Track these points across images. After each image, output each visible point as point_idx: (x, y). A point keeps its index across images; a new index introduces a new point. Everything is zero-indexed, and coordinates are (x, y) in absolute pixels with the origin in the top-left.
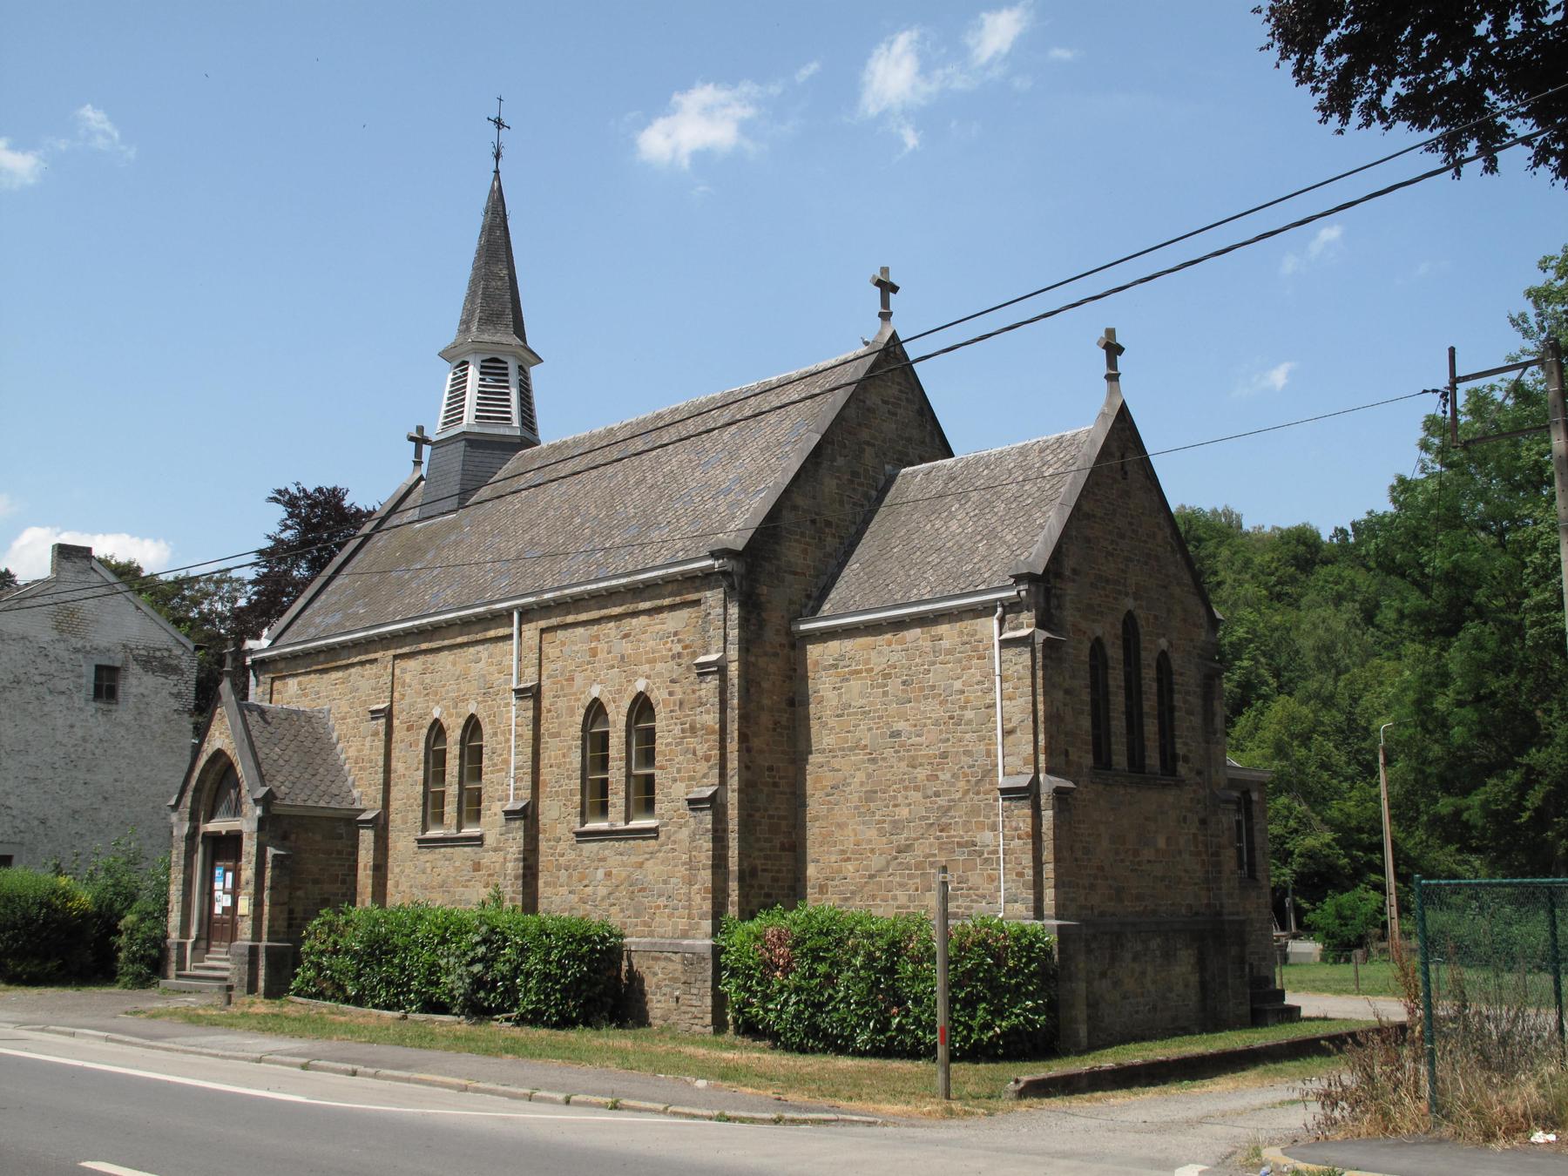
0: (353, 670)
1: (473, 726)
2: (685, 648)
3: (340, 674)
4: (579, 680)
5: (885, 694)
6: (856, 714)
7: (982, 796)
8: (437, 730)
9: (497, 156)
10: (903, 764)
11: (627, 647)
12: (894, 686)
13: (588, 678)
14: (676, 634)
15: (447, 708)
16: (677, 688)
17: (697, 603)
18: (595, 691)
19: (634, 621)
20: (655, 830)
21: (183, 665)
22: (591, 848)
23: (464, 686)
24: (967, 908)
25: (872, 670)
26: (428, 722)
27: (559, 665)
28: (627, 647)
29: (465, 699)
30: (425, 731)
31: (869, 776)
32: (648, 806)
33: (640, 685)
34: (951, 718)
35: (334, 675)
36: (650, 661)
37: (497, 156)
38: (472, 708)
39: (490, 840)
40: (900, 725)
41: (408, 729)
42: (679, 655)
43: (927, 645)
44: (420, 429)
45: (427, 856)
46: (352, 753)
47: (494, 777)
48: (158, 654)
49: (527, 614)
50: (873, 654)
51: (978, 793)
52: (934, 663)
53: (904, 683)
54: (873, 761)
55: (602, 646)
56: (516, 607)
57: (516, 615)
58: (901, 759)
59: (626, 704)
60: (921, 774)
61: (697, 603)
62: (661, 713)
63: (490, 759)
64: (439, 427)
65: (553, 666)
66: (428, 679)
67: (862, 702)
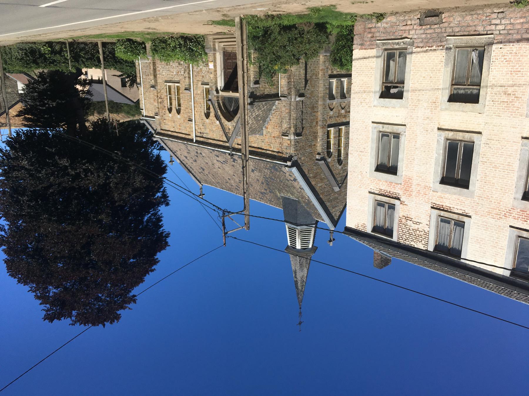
1: (207, 115)
9: (300, 313)
15: (215, 123)
17: (161, 129)
18: (179, 116)
28: (173, 124)
33: (170, 115)
35: (256, 145)
37: (300, 313)
38: (207, 121)
39: (200, 83)
49: (191, 140)
57: (194, 141)
61: (161, 129)
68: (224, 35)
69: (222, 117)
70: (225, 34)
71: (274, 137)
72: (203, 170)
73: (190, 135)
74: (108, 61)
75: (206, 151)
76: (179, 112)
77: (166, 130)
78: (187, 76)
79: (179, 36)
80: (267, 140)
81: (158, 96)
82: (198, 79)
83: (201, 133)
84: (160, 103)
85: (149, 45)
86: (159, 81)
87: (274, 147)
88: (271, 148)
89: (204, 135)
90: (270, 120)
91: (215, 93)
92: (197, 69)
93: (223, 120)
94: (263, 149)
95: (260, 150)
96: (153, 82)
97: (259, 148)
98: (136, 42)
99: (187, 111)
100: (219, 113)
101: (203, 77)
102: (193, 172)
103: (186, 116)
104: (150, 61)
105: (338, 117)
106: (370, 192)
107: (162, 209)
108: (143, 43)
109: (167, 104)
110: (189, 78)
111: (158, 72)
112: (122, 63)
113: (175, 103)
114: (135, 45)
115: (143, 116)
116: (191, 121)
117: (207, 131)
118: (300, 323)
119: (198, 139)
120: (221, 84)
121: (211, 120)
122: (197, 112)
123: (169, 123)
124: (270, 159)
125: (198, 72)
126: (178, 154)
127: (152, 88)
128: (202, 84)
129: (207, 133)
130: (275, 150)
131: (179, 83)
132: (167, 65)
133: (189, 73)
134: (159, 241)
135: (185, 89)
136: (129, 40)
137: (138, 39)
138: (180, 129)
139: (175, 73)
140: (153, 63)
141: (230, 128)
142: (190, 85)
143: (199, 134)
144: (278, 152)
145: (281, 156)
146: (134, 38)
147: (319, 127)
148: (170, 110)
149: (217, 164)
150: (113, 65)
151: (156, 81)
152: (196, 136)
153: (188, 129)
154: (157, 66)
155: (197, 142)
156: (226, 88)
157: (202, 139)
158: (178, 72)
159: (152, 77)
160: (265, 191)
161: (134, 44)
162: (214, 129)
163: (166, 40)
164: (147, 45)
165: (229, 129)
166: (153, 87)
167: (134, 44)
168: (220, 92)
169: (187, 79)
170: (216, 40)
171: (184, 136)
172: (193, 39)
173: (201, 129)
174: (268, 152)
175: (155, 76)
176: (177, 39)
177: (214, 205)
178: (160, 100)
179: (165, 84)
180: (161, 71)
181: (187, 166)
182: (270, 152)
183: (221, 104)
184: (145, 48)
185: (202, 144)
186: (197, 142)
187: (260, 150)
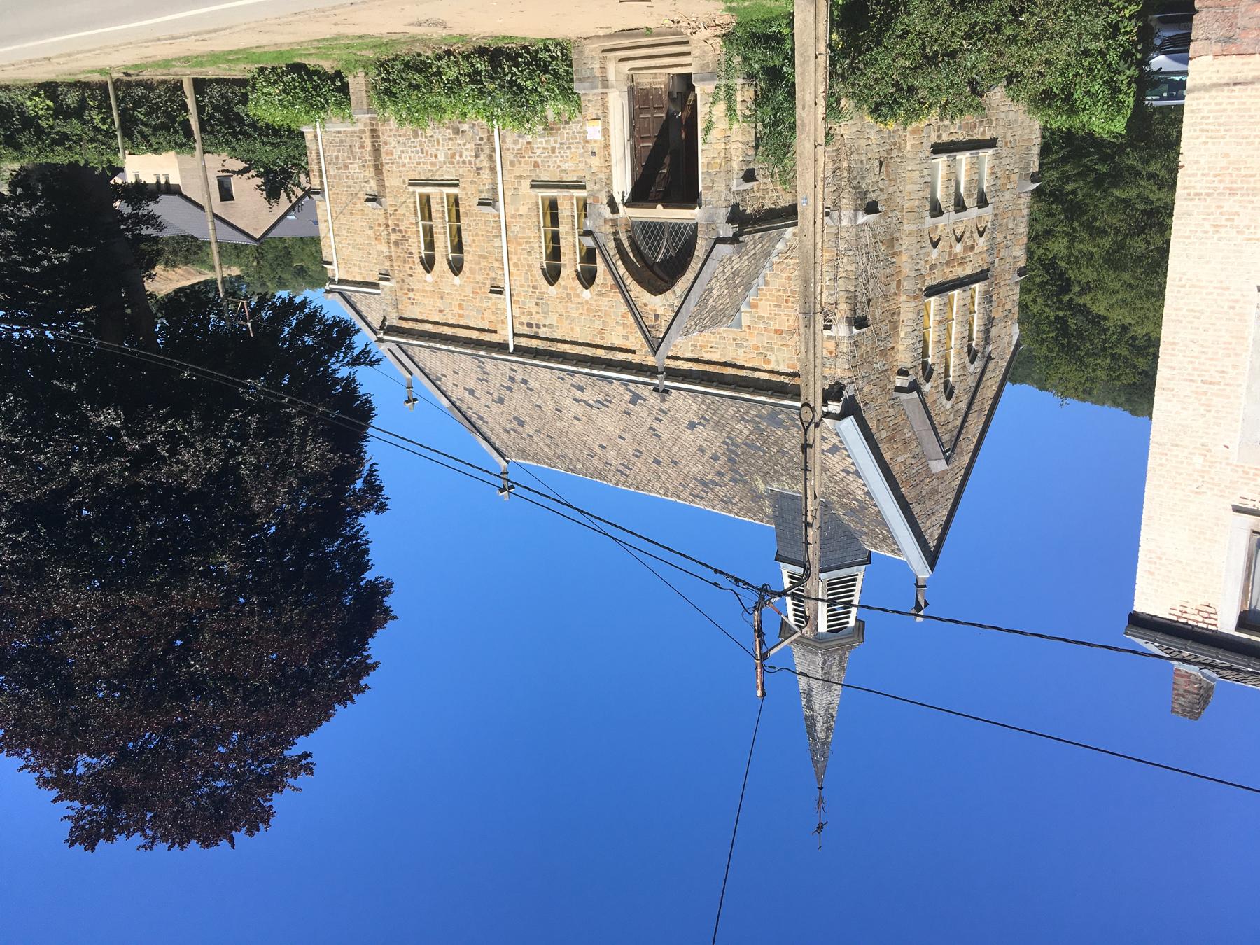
0: (689, 355)
1: (552, 275)
3: (707, 357)
9: (820, 801)
15: (578, 296)
17: (401, 318)
18: (457, 280)
19: (437, 320)
20: (410, 185)
26: (595, 288)
27: (485, 305)
33: (429, 277)
35: (715, 357)
37: (820, 801)
38: (552, 290)
39: (526, 184)
49: (502, 347)
57: (511, 349)
61: (401, 318)
65: (490, 305)
66: (598, 324)
68: (647, 36)
69: (629, 281)
70: (649, 32)
71: (777, 331)
72: (521, 423)
73: (495, 332)
74: (212, 132)
75: (542, 375)
76: (456, 267)
77: (416, 320)
78: (486, 164)
79: (471, 49)
80: (754, 341)
81: (387, 226)
82: (518, 171)
83: (530, 325)
84: (396, 244)
85: (357, 82)
86: (392, 181)
87: (781, 360)
88: (769, 362)
89: (542, 332)
90: (767, 283)
91: (607, 212)
92: (516, 142)
93: (636, 290)
94: (742, 367)
95: (730, 371)
96: (372, 187)
97: (726, 364)
98: (316, 72)
99: (484, 262)
100: (622, 270)
101: (536, 165)
102: (484, 429)
103: (480, 278)
104: (360, 126)
105: (947, 264)
106: (1237, 510)
107: (370, 522)
108: (338, 74)
109: (417, 246)
110: (493, 169)
111: (385, 158)
112: (250, 136)
113: (443, 245)
114: (315, 84)
115: (332, 281)
116: (501, 293)
117: (552, 319)
118: (820, 827)
119: (523, 342)
120: (622, 184)
121: (565, 288)
122: (516, 265)
123: (426, 301)
124: (771, 396)
125: (519, 152)
126: (448, 384)
127: (369, 204)
128: (533, 186)
129: (551, 326)
130: (782, 369)
131: (457, 185)
132: (416, 135)
133: (491, 157)
134: (371, 608)
135: (480, 204)
136: (298, 68)
137: (328, 66)
138: (461, 316)
139: (441, 158)
140: (373, 131)
141: (660, 312)
142: (495, 190)
143: (524, 330)
146: (311, 62)
147: (903, 298)
148: (428, 264)
149: (573, 409)
150: (228, 142)
151: (381, 183)
152: (515, 335)
153: (488, 314)
154: (382, 139)
155: (519, 350)
156: (640, 196)
157: (534, 343)
158: (453, 156)
159: (370, 172)
160: (717, 479)
161: (311, 80)
162: (574, 313)
163: (423, 63)
164: (350, 80)
165: (656, 316)
166: (373, 199)
167: (311, 80)
168: (621, 207)
169: (486, 175)
170: (609, 55)
171: (475, 335)
172: (521, 56)
173: (530, 313)
174: (757, 375)
175: (378, 169)
176: (467, 57)
177: (716, 571)
178: (393, 237)
179: (411, 189)
180: (397, 153)
181: (469, 413)
182: (766, 376)
183: (626, 244)
184: (345, 89)
185: (535, 358)
186: (519, 350)
187: (730, 371)
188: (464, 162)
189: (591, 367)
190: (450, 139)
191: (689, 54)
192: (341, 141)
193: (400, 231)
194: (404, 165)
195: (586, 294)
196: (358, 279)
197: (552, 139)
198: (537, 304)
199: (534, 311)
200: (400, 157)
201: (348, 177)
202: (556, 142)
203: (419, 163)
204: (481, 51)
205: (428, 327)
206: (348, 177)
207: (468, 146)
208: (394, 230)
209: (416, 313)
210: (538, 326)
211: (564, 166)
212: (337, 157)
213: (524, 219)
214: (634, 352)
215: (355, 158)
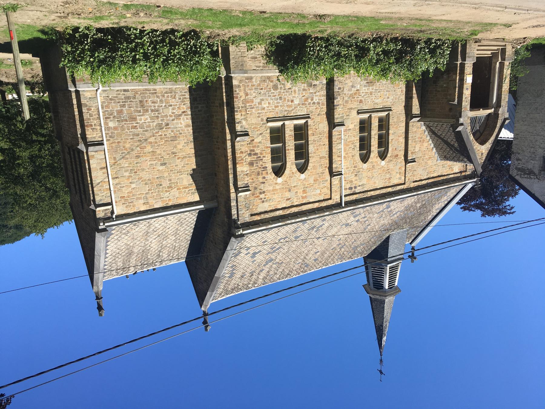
0: (425, 177)
1: (365, 158)
2: (258, 197)
3: (432, 176)
4: (311, 181)
5: (170, 180)
6: (185, 171)
7: (116, 141)
8: (383, 156)
10: (158, 152)
11: (288, 195)
12: (166, 184)
13: (306, 181)
14: (263, 202)
16: (261, 180)
17: (252, 215)
18: (303, 176)
19: (284, 206)
20: (268, 121)
21: (516, 171)
22: (303, 112)
23: (370, 174)
24: (120, 94)
25: (178, 189)
27: (322, 186)
28: (288, 195)
29: (369, 170)
30: (389, 155)
31: (175, 147)
32: (273, 131)
33: (280, 180)
34: (136, 172)
35: (435, 175)
36: (276, 190)
38: (365, 166)
39: (354, 112)
40: (161, 168)
41: (397, 155)
42: (261, 193)
43: (151, 201)
44: (412, 261)
45: (388, 104)
46: (425, 144)
47: (353, 139)
48: (526, 176)
49: (338, 205)
50: (177, 195)
51: (119, 142)
52: (147, 193)
53: (161, 185)
54: (173, 153)
55: (300, 194)
56: (343, 208)
57: (343, 205)
58: (160, 154)
59: (287, 172)
60: (149, 149)
61: (252, 215)
62: (270, 170)
63: (355, 146)
64: (400, 265)
65: (325, 185)
66: (388, 176)
67: (182, 176)
82: (350, 105)
84: (251, 164)
94: (444, 176)
95: (442, 178)
101: (361, 101)
117: (364, 181)
123: (275, 197)
125: (351, 95)
129: (363, 185)
139: (296, 102)
141: (484, 152)
144: (461, 172)
145: (465, 175)
155: (348, 204)
157: (354, 197)
158: (306, 100)
171: (316, 205)
173: (352, 181)
178: (249, 159)
182: (452, 176)
186: (348, 204)
187: (442, 178)
188: (314, 103)
189: (371, 201)
190: (304, 90)
191: (477, 50)
192: (128, 98)
193: (256, 154)
194: (264, 109)
195: (383, 163)
196: (143, 208)
197: (371, 88)
198: (356, 175)
199: (353, 180)
200: (260, 103)
201: (135, 127)
202: (372, 89)
203: (278, 107)
204: (395, 40)
205: (278, 213)
206: (135, 127)
207: (317, 94)
208: (250, 155)
209: (266, 207)
210: (355, 187)
211: (376, 101)
212: (120, 112)
213: (351, 131)
214: (404, 184)
215: (147, 111)
